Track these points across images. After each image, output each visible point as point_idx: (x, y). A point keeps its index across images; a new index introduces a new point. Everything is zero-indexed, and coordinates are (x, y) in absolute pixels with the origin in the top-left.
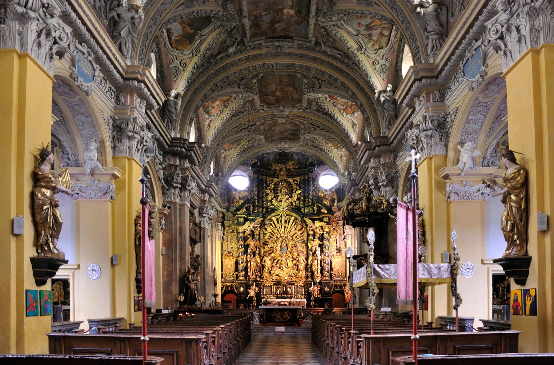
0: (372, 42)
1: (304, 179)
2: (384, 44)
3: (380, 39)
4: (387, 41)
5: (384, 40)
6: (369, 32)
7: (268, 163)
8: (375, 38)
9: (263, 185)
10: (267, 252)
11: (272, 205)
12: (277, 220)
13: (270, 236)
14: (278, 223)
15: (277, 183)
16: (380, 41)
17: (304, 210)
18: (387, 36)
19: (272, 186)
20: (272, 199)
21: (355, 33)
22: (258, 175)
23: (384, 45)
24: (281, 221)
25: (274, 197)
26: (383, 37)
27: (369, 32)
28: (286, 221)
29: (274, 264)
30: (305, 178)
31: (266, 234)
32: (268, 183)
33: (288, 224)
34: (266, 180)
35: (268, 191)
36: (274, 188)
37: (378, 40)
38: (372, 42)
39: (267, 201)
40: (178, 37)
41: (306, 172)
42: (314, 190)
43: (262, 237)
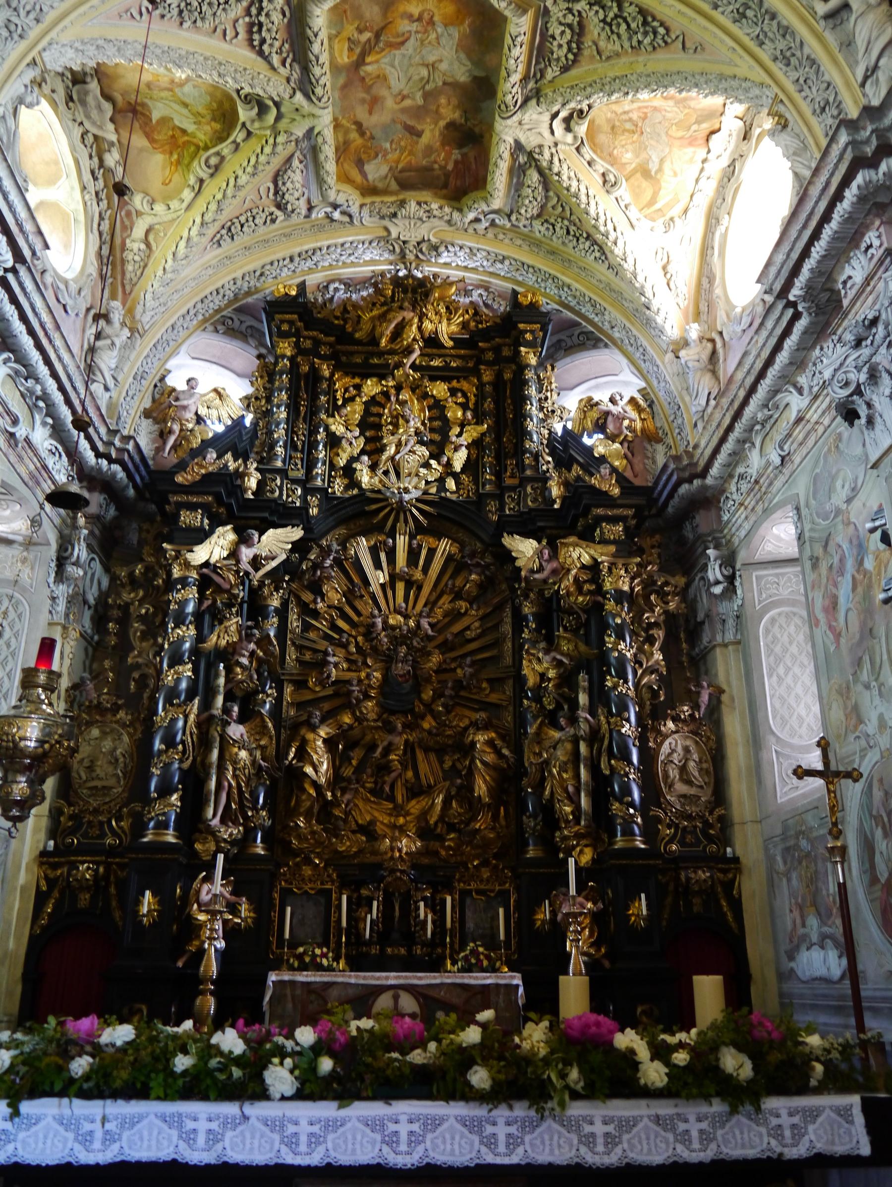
1: (498, 383)
7: (345, 310)
9: (314, 397)
10: (315, 702)
11: (353, 482)
12: (374, 552)
13: (334, 627)
14: (378, 566)
15: (379, 398)
17: (501, 508)
19: (356, 410)
20: (353, 459)
22: (300, 350)
24: (391, 554)
25: (363, 452)
28: (413, 555)
29: (348, 772)
30: (499, 375)
31: (316, 614)
32: (339, 395)
33: (425, 570)
34: (331, 381)
35: (338, 428)
36: (363, 418)
39: (332, 466)
41: (506, 352)
42: (543, 420)
43: (294, 621)
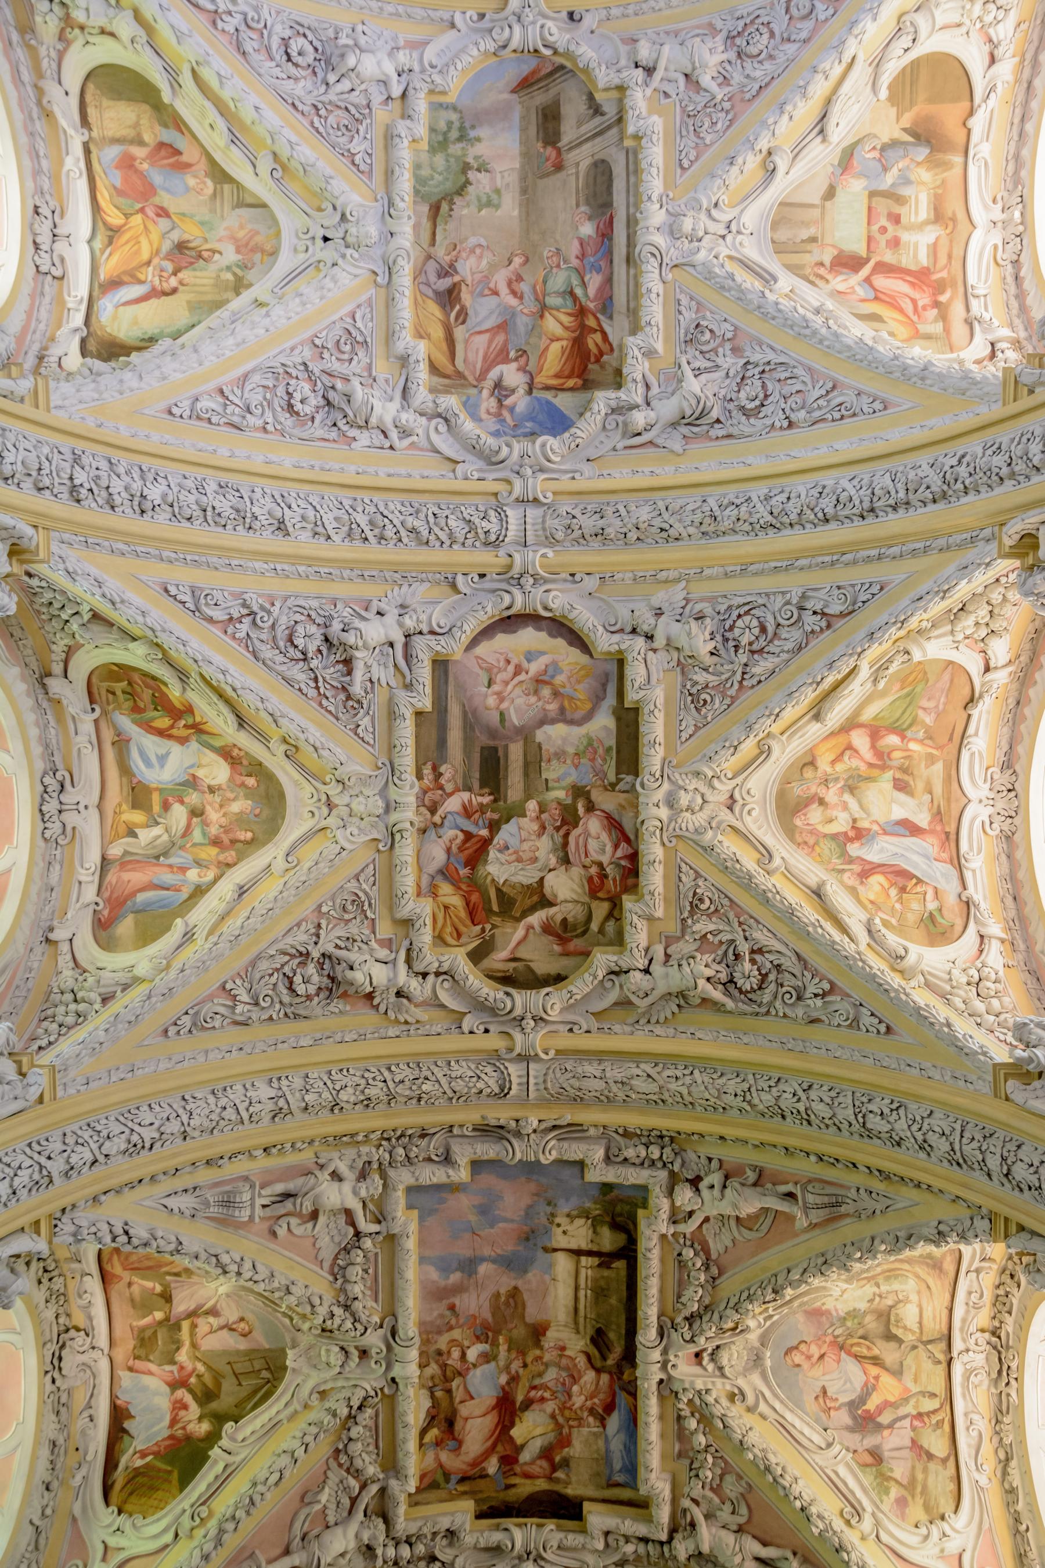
0: (894, 1492)
2: (942, 1501)
3: (920, 1476)
4: (952, 1486)
5: (939, 1480)
6: (870, 1441)
8: (899, 1470)
16: (925, 1487)
18: (944, 1461)
21: (817, 1439)
23: (946, 1505)
26: (932, 1466)
27: (870, 1441)
37: (913, 1480)
38: (894, 1492)
40: (143, 1454)
